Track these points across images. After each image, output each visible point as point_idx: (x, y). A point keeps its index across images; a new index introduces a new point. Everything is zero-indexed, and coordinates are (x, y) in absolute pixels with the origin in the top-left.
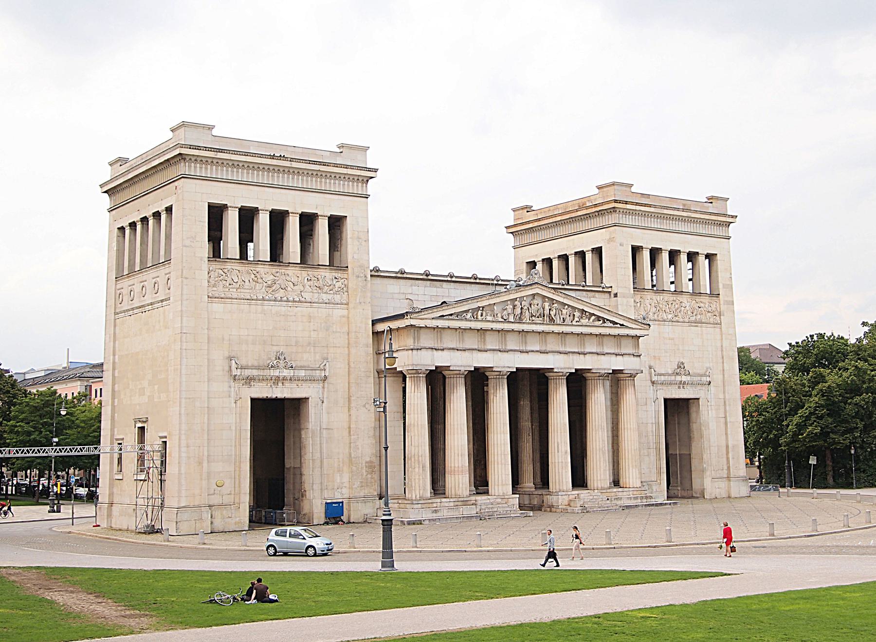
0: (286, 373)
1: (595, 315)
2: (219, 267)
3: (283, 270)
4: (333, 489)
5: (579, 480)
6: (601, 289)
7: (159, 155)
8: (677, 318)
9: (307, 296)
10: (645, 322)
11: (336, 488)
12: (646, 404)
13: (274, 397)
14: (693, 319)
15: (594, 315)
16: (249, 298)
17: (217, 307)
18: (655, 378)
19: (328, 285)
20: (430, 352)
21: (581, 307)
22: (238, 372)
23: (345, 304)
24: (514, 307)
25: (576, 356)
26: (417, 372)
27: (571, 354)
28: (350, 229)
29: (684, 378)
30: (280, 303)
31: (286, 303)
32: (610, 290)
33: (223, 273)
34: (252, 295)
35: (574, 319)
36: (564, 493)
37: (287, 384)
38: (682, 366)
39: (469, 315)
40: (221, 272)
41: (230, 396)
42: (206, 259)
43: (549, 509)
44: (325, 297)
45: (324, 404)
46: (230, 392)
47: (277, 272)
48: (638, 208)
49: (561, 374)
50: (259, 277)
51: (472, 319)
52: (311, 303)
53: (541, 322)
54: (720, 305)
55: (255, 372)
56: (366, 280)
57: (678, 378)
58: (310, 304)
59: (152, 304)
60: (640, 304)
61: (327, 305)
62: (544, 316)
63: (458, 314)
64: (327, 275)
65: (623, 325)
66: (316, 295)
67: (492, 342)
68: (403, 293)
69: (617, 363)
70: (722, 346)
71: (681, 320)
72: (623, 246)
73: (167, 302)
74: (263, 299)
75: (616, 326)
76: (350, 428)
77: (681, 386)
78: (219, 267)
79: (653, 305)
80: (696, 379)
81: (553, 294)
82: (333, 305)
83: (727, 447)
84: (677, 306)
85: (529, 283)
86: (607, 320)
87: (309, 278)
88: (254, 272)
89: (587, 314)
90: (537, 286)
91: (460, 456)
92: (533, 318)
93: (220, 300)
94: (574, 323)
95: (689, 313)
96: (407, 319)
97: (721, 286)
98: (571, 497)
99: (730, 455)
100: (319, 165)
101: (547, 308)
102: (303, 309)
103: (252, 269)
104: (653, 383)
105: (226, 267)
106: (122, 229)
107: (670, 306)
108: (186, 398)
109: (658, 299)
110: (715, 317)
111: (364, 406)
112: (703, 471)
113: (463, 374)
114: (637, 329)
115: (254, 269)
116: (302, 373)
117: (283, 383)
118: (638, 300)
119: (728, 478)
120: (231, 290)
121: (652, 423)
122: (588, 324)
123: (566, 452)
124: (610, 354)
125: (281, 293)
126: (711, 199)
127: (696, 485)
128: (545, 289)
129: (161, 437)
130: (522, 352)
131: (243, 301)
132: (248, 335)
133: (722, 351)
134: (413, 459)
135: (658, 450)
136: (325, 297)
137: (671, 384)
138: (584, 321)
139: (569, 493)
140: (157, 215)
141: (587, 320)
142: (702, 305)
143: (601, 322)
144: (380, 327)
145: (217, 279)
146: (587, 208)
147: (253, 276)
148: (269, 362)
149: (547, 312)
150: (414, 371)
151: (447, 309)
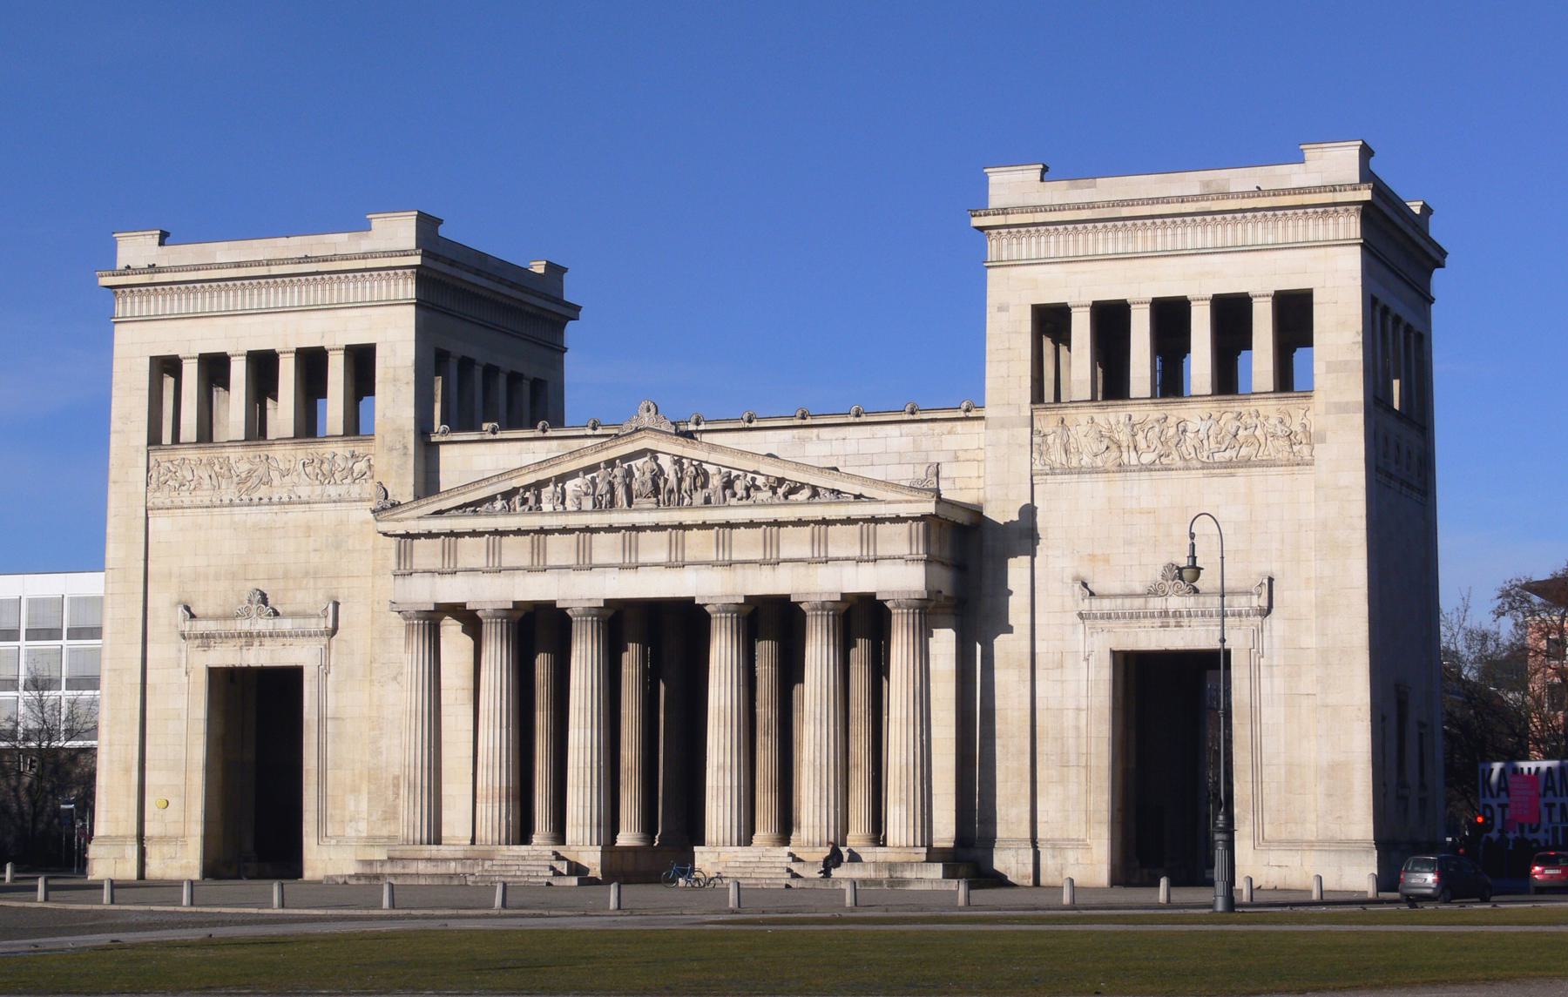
6: (961, 414)
9: (304, 492)
11: (347, 818)
12: (1062, 666)
13: (245, 665)
14: (1228, 455)
16: (208, 503)
18: (1085, 606)
19: (340, 469)
20: (427, 578)
22: (187, 626)
29: (1175, 603)
39: (499, 504)
40: (169, 464)
46: (179, 658)
52: (308, 503)
56: (405, 454)
57: (1156, 604)
58: (307, 506)
64: (341, 449)
66: (318, 489)
74: (231, 504)
77: (1172, 621)
82: (347, 504)
94: (734, 501)
100: (315, 262)
102: (296, 515)
105: (178, 457)
108: (110, 670)
109: (1113, 422)
111: (395, 678)
114: (900, 502)
115: (219, 455)
116: (286, 625)
121: (1078, 709)
124: (837, 559)
125: (263, 491)
130: (622, 567)
132: (208, 566)
136: (333, 491)
137: (1134, 616)
141: (770, 494)
147: (217, 468)
151: (447, 498)
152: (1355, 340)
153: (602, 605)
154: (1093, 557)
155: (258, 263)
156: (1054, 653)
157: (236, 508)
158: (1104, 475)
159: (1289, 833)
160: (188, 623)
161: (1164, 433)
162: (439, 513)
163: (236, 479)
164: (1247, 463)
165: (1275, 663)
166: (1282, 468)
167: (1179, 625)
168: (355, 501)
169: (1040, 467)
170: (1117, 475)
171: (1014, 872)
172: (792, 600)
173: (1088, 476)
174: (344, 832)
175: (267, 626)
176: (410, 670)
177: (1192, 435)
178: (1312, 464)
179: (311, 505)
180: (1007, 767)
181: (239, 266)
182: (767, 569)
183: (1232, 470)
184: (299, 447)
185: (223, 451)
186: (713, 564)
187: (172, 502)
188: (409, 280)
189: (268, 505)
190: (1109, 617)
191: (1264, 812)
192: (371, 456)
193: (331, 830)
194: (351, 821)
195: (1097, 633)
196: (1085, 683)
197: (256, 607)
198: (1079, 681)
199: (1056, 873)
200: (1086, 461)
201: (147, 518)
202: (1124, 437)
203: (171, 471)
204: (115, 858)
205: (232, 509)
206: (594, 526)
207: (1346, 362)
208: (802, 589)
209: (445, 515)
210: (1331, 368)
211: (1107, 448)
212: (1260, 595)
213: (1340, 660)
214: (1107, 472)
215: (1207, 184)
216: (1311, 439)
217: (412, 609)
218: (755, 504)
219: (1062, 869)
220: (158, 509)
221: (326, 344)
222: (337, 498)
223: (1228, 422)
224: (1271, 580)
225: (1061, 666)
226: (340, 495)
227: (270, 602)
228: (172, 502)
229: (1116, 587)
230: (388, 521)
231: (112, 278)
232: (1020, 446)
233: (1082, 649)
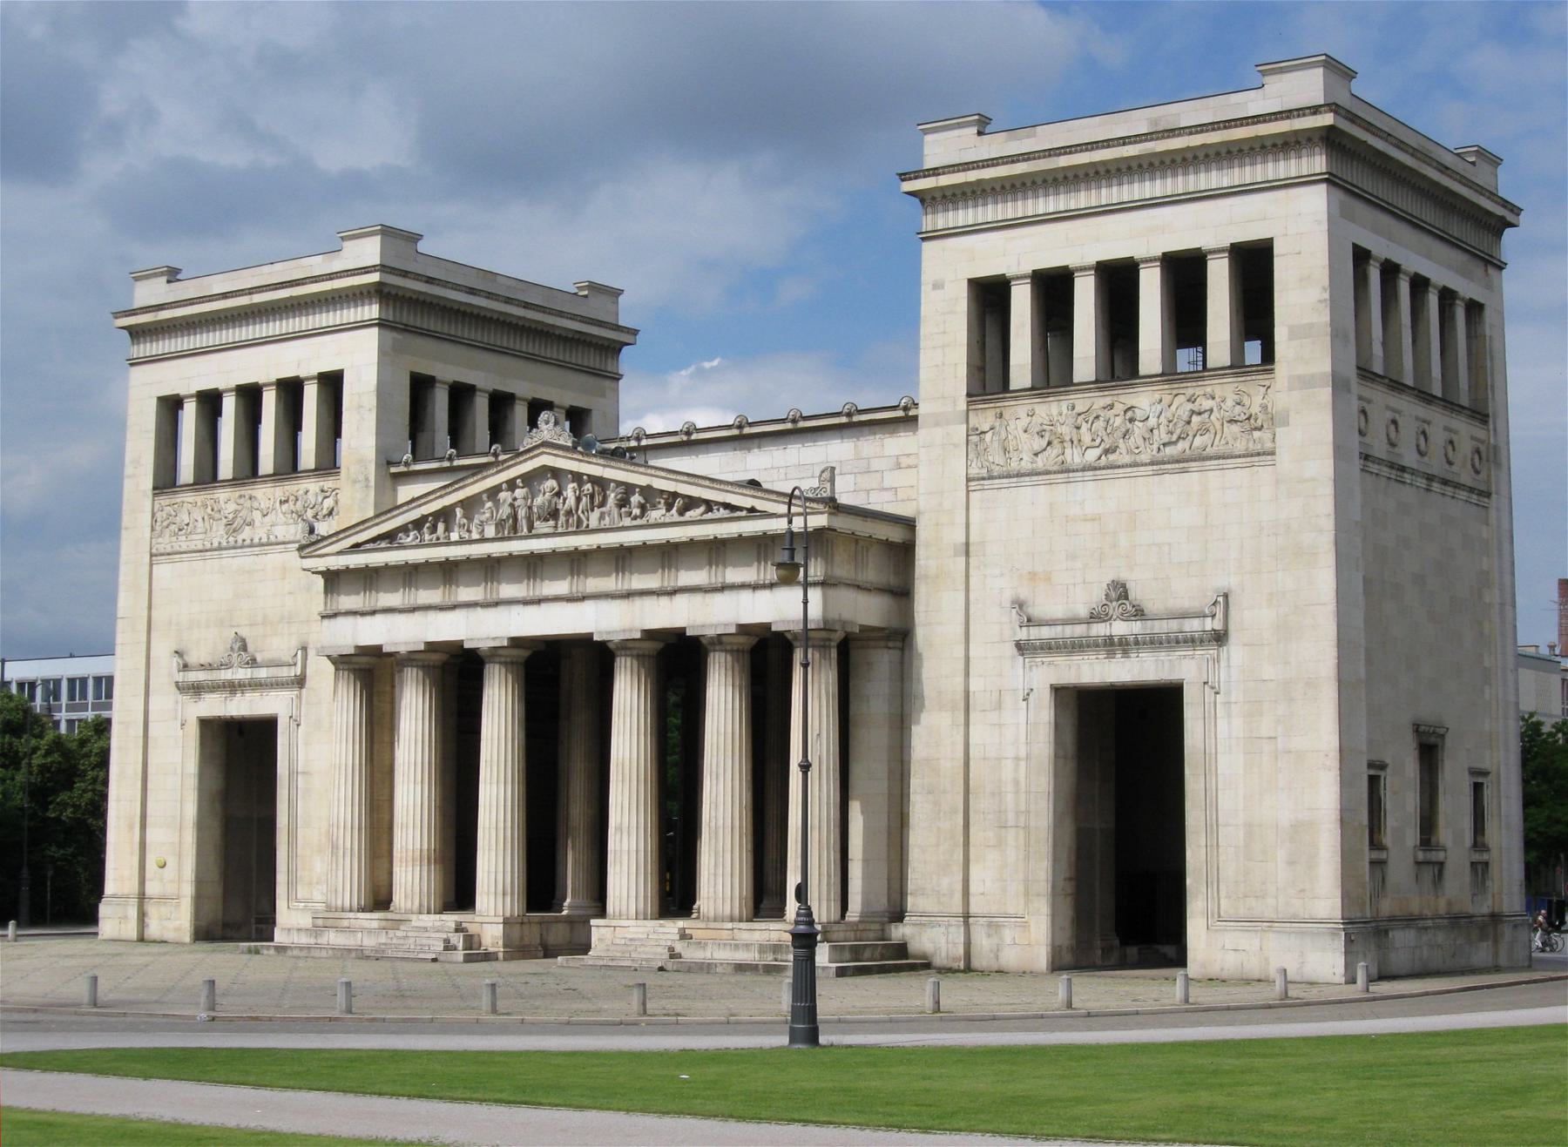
0: (242, 674)
1: (684, 497)
2: (168, 502)
3: (250, 492)
4: (310, 884)
8: (1112, 457)
11: (315, 881)
12: (1000, 707)
16: (200, 547)
17: (163, 571)
18: (1023, 634)
19: (311, 506)
20: (350, 620)
25: (649, 602)
29: (1119, 628)
34: (205, 543)
42: (150, 494)
45: (300, 727)
46: (176, 710)
47: (241, 496)
52: (284, 543)
55: (200, 676)
57: (1100, 630)
58: (283, 546)
65: (752, 510)
71: (1127, 459)
74: (220, 548)
75: (738, 514)
78: (168, 502)
80: (1160, 627)
90: (542, 450)
93: (167, 557)
94: (627, 522)
109: (1055, 411)
110: (1256, 434)
116: (262, 673)
121: (1017, 759)
122: (662, 521)
125: (246, 534)
128: (561, 453)
142: (1207, 404)
143: (702, 509)
152: (1322, 298)
153: (506, 644)
154: (1033, 576)
156: (991, 691)
158: (1044, 477)
159: (1249, 909)
161: (1111, 422)
162: (356, 547)
163: (224, 521)
165: (1233, 700)
166: (1240, 460)
167: (1126, 653)
169: (976, 471)
170: (1060, 476)
171: (944, 954)
172: (688, 634)
173: (1027, 479)
174: (312, 895)
175: (246, 674)
176: (339, 721)
177: (1142, 424)
178: (1273, 453)
180: (939, 828)
182: (664, 600)
183: (1185, 465)
184: (277, 484)
185: (215, 491)
187: (172, 547)
188: (374, 300)
190: (1050, 648)
191: (1220, 884)
193: (302, 892)
194: (317, 883)
195: (1037, 666)
196: (1025, 725)
198: (1018, 724)
199: (992, 955)
200: (1026, 465)
201: (151, 565)
202: (1066, 431)
206: (495, 555)
207: (1311, 326)
210: (1294, 333)
211: (1049, 443)
213: (1305, 694)
214: (1048, 473)
215: (1155, 122)
217: (335, 654)
219: (998, 950)
220: (162, 555)
221: (302, 375)
223: (1182, 407)
224: (1226, 596)
225: (999, 706)
227: (251, 648)
228: (172, 547)
229: (1058, 611)
232: (956, 446)
233: (1021, 687)
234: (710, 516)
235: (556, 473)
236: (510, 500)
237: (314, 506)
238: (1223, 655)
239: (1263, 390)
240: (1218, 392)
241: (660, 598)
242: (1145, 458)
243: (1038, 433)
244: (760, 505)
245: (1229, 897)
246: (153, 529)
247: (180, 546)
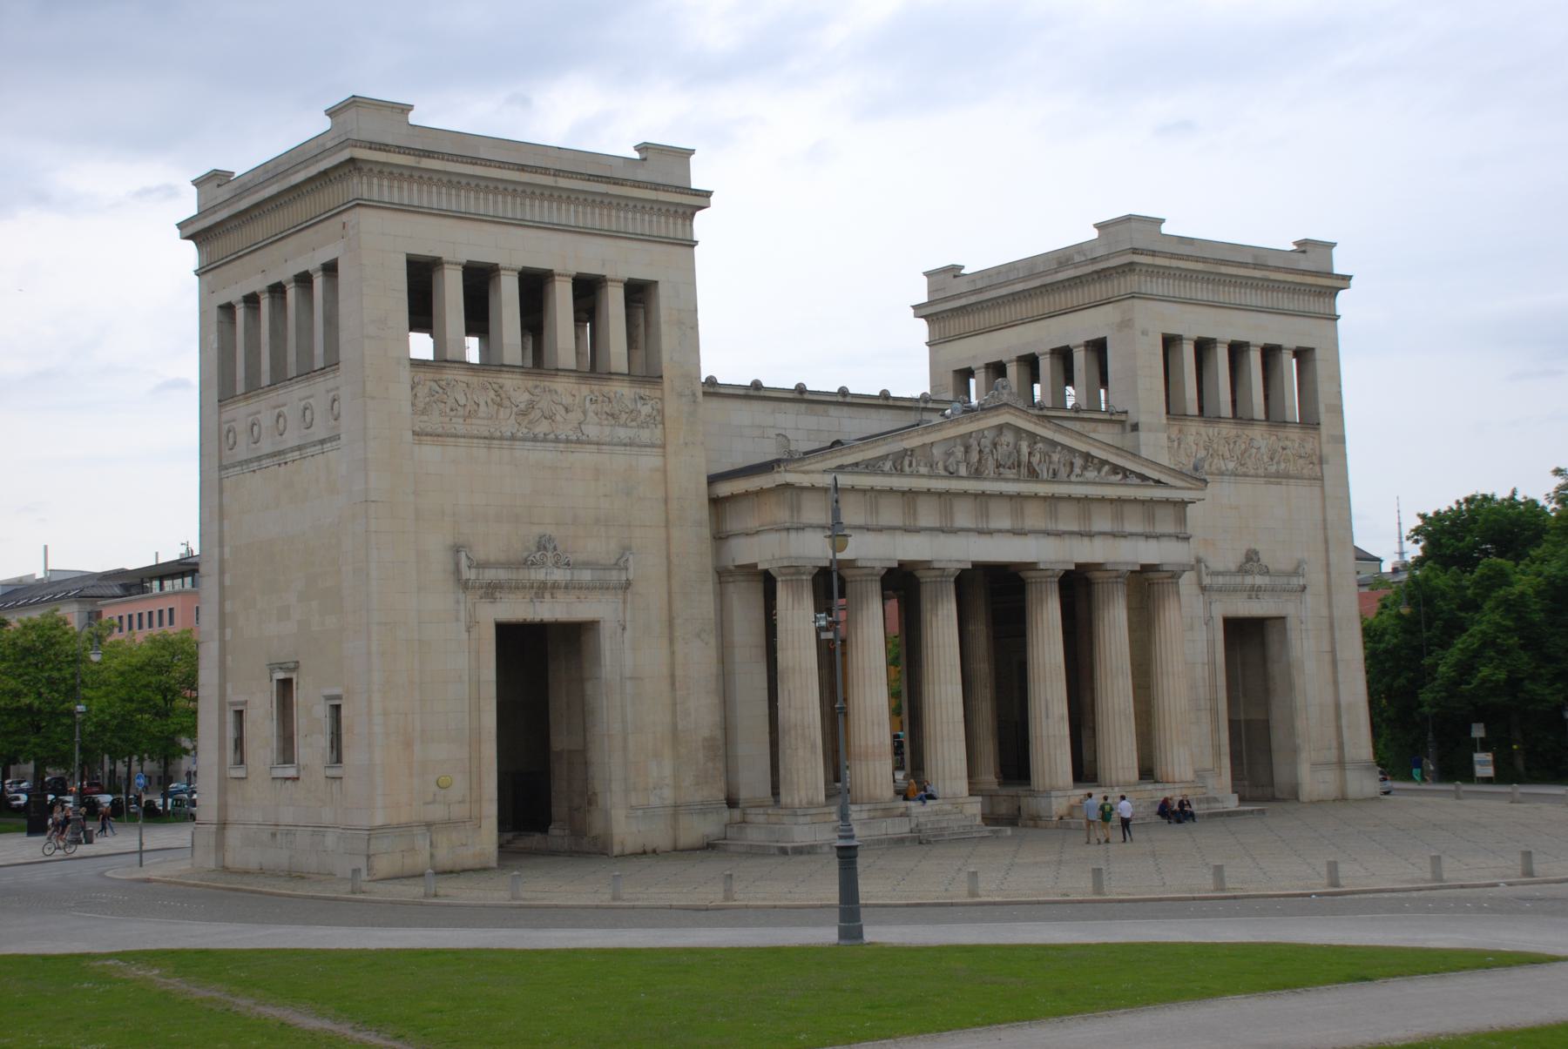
0: (559, 575)
2: (429, 376)
3: (546, 383)
5: (1085, 771)
7: (306, 163)
9: (592, 431)
10: (1197, 475)
13: (537, 618)
14: (1273, 469)
15: (1104, 462)
16: (486, 434)
17: (430, 453)
18: (1207, 581)
19: (627, 410)
21: (1083, 447)
23: (660, 447)
24: (967, 449)
26: (796, 570)
27: (1066, 536)
28: (665, 302)
29: (1259, 580)
30: (542, 444)
31: (554, 445)
32: (1123, 417)
33: (438, 388)
34: (492, 430)
35: (1072, 471)
36: (1060, 793)
37: (560, 595)
38: (1255, 559)
41: (457, 620)
43: (1031, 823)
44: (622, 433)
47: (536, 387)
48: (1175, 263)
49: (1050, 573)
50: (503, 396)
51: (894, 471)
52: (598, 444)
53: (1016, 477)
54: (1320, 443)
55: (502, 575)
56: (694, 402)
57: (1249, 580)
58: (596, 447)
59: (300, 448)
60: (1179, 444)
61: (628, 448)
62: (1019, 466)
63: (871, 467)
64: (623, 391)
65: (1158, 482)
66: (607, 430)
67: (928, 515)
68: (759, 426)
69: (1149, 552)
70: (1325, 520)
72: (1147, 335)
73: (334, 443)
74: (513, 438)
76: (673, 676)
79: (1201, 444)
81: (1036, 424)
82: (637, 449)
83: (1337, 706)
84: (1243, 447)
85: (992, 405)
86: (1132, 472)
87: (594, 398)
88: (495, 386)
89: (1096, 461)
91: (876, 727)
92: (1001, 470)
93: (435, 439)
94: (1073, 478)
95: (1266, 459)
96: (778, 472)
97: (1322, 408)
98: (1074, 801)
99: (1344, 722)
101: (1025, 449)
102: (585, 458)
103: (490, 380)
104: (1203, 589)
105: (445, 377)
106: (228, 309)
107: (1232, 446)
109: (1211, 434)
110: (1311, 466)
111: (698, 635)
112: (1295, 751)
113: (878, 575)
116: (586, 576)
117: (552, 594)
118: (1173, 436)
119: (1341, 763)
120: (454, 420)
121: (1204, 664)
122: (1097, 480)
123: (1063, 718)
126: (1304, 246)
127: (1281, 775)
129: (328, 698)
130: (981, 532)
131: (475, 441)
133: (1325, 528)
134: (793, 733)
135: (1214, 712)
136: (622, 433)
137: (1235, 590)
138: (1091, 474)
139: (1069, 793)
140: (304, 280)
141: (1096, 473)
142: (1288, 443)
143: (1120, 476)
144: (725, 489)
145: (428, 399)
146: (1077, 265)
147: (492, 394)
148: (525, 554)
149: (1025, 458)
150: (792, 570)
151: (849, 454)
155: (545, 171)
157: (517, 443)
160: (473, 571)
163: (515, 409)
164: (1288, 476)
168: (646, 446)
179: (601, 447)
181: (523, 170)
182: (1086, 541)
186: (1048, 533)
187: (443, 428)
189: (552, 441)
190: (1221, 591)
192: (657, 400)
194: (655, 789)
197: (552, 555)
203: (437, 392)
204: (403, 851)
205: (512, 442)
208: (1112, 560)
209: (846, 470)
212: (1303, 576)
216: (1321, 461)
218: (1086, 483)
220: (427, 435)
222: (627, 440)
226: (630, 438)
228: (443, 428)
230: (796, 472)
231: (368, 151)
234: (1128, 481)
235: (1018, 431)
236: (978, 449)
237: (632, 412)
238: (1303, 600)
239: (1311, 439)
240: (1292, 436)
241: (1084, 538)
242: (1261, 472)
243: (1204, 447)
244: (1164, 478)
245: (1314, 750)
246: (413, 405)
247: (455, 428)
